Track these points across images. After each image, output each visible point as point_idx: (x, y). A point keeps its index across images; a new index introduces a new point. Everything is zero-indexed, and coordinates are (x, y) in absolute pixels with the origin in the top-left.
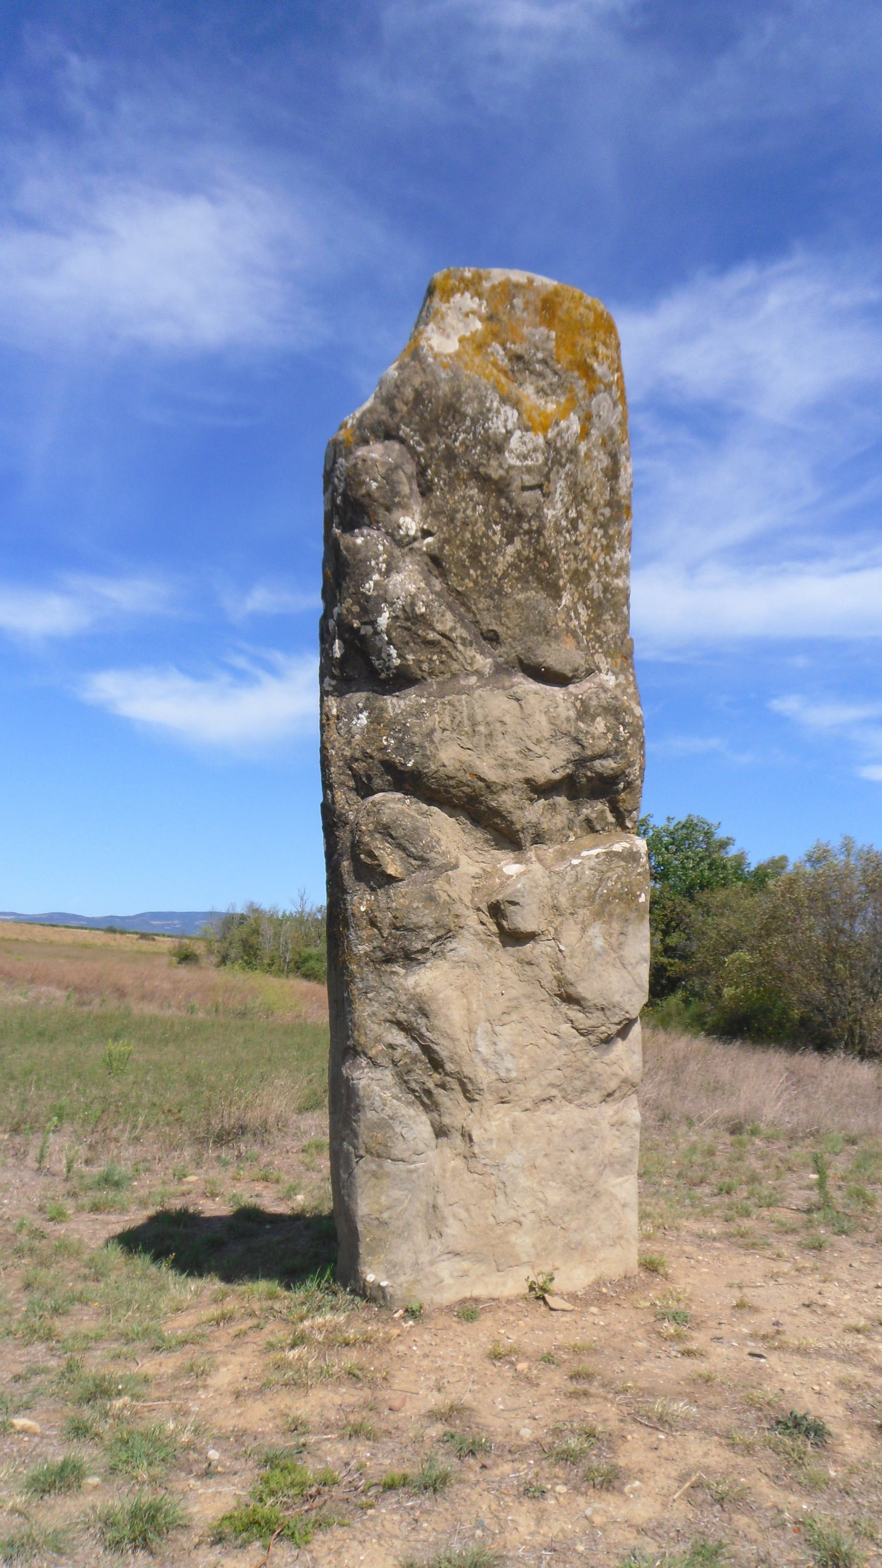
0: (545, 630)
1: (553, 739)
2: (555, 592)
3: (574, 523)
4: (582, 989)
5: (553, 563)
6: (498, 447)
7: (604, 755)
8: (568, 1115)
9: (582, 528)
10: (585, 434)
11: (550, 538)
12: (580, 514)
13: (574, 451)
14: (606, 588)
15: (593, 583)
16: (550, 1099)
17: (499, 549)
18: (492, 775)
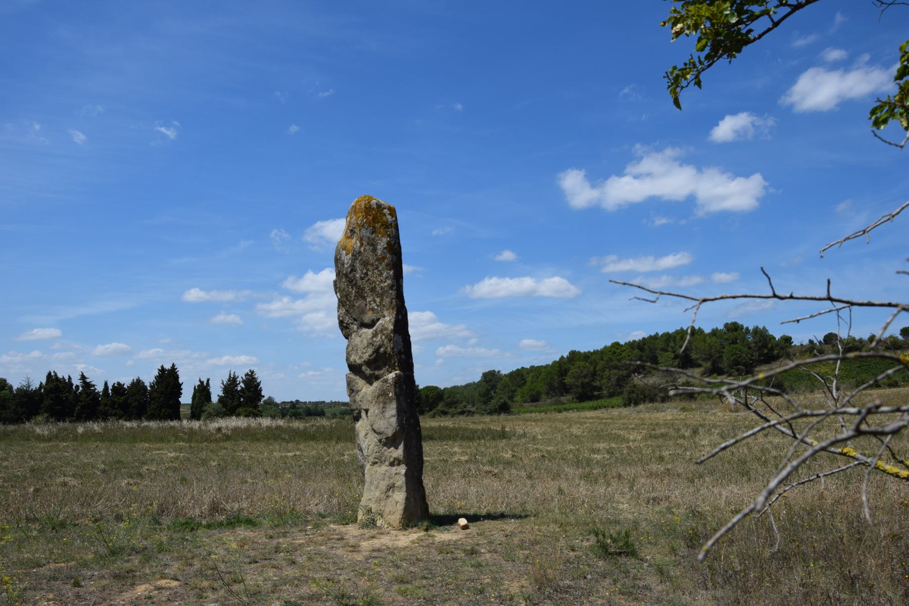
0: (363, 312)
1: (368, 346)
2: (364, 298)
3: (366, 274)
4: (376, 427)
5: (363, 289)
6: (343, 264)
7: (380, 347)
8: (384, 468)
9: (370, 273)
10: (362, 245)
11: (360, 283)
12: (368, 270)
13: (360, 252)
14: (382, 288)
15: (378, 289)
16: (376, 463)
17: (351, 293)
18: (359, 362)
